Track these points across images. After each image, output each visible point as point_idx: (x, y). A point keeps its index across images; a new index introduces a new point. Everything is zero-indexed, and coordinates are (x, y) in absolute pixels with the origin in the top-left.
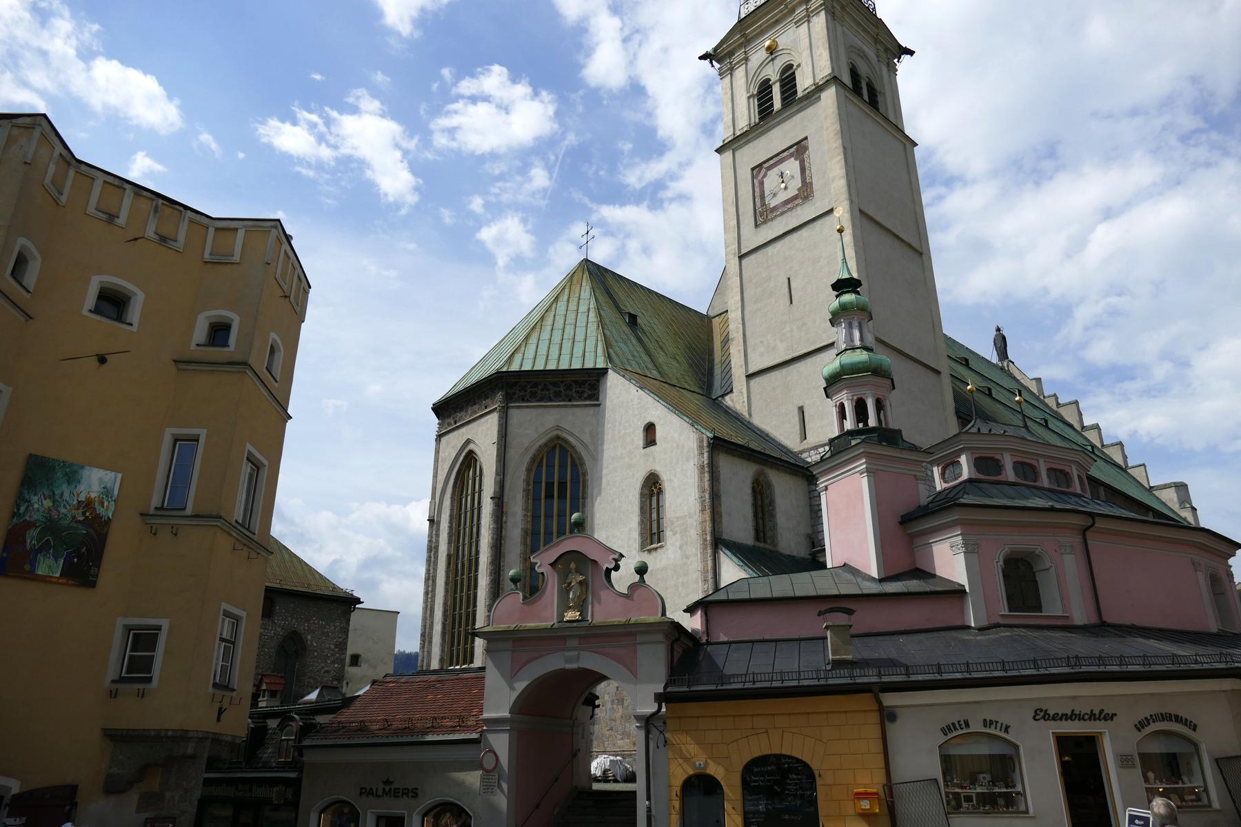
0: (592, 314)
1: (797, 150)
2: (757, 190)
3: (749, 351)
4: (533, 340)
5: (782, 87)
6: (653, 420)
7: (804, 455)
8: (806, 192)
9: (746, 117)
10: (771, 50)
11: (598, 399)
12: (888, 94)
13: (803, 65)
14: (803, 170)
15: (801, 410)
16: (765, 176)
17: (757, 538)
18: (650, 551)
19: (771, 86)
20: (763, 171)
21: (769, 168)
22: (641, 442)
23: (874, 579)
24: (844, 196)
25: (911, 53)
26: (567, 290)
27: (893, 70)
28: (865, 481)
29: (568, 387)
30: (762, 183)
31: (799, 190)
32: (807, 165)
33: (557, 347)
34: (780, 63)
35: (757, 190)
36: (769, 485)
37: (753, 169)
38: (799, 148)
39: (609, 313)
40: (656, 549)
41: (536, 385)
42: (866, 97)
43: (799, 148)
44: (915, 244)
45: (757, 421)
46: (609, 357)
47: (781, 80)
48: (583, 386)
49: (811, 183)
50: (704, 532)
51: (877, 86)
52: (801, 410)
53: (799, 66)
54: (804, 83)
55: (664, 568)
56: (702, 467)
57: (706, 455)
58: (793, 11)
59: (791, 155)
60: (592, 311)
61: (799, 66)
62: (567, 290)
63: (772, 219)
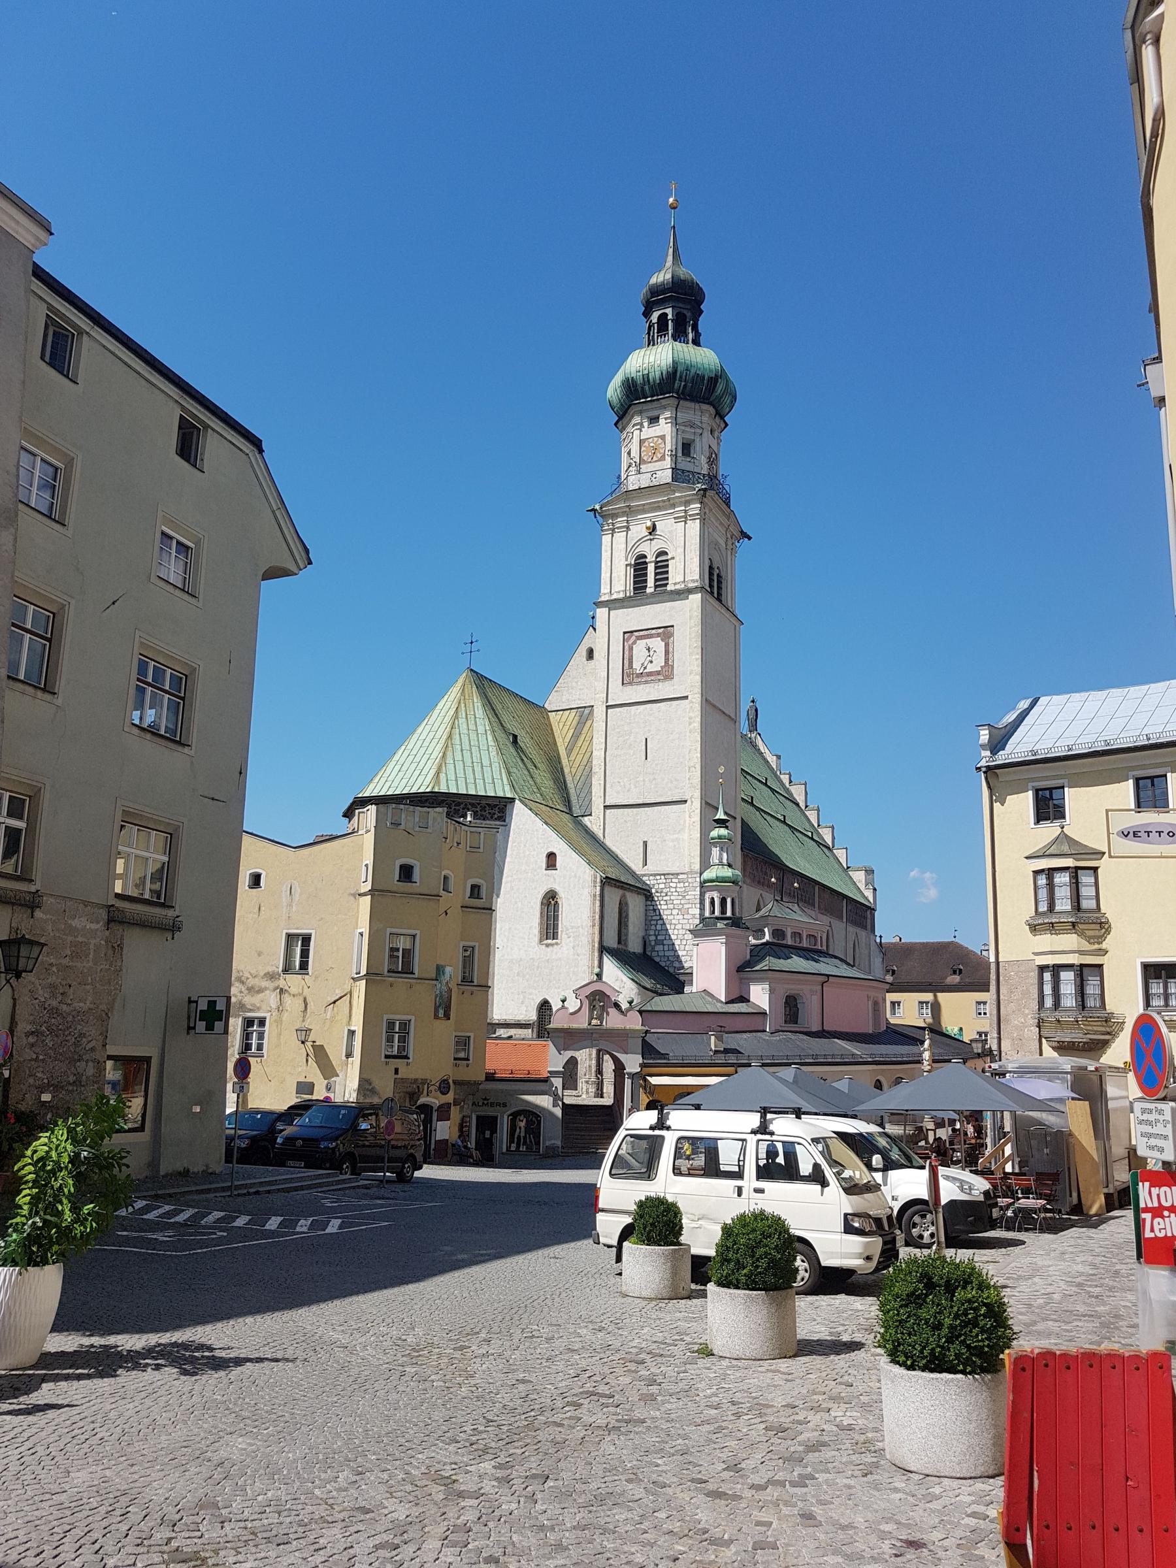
0: (490, 738)
2: (627, 653)
4: (449, 760)
5: (656, 568)
7: (645, 878)
8: (666, 673)
9: (623, 582)
10: (653, 530)
13: (677, 559)
14: (667, 652)
15: (645, 843)
16: (634, 643)
17: (619, 942)
18: (547, 945)
20: (633, 638)
21: (639, 638)
22: (544, 865)
24: (698, 690)
25: (750, 538)
27: (733, 551)
29: (483, 809)
30: (631, 649)
34: (657, 545)
35: (627, 653)
36: (627, 904)
40: (552, 945)
41: (459, 804)
44: (733, 716)
45: (609, 842)
47: (656, 562)
48: (495, 810)
50: (593, 941)
51: (723, 574)
52: (645, 843)
54: (675, 578)
56: (595, 896)
57: (598, 888)
58: (673, 506)
59: (658, 635)
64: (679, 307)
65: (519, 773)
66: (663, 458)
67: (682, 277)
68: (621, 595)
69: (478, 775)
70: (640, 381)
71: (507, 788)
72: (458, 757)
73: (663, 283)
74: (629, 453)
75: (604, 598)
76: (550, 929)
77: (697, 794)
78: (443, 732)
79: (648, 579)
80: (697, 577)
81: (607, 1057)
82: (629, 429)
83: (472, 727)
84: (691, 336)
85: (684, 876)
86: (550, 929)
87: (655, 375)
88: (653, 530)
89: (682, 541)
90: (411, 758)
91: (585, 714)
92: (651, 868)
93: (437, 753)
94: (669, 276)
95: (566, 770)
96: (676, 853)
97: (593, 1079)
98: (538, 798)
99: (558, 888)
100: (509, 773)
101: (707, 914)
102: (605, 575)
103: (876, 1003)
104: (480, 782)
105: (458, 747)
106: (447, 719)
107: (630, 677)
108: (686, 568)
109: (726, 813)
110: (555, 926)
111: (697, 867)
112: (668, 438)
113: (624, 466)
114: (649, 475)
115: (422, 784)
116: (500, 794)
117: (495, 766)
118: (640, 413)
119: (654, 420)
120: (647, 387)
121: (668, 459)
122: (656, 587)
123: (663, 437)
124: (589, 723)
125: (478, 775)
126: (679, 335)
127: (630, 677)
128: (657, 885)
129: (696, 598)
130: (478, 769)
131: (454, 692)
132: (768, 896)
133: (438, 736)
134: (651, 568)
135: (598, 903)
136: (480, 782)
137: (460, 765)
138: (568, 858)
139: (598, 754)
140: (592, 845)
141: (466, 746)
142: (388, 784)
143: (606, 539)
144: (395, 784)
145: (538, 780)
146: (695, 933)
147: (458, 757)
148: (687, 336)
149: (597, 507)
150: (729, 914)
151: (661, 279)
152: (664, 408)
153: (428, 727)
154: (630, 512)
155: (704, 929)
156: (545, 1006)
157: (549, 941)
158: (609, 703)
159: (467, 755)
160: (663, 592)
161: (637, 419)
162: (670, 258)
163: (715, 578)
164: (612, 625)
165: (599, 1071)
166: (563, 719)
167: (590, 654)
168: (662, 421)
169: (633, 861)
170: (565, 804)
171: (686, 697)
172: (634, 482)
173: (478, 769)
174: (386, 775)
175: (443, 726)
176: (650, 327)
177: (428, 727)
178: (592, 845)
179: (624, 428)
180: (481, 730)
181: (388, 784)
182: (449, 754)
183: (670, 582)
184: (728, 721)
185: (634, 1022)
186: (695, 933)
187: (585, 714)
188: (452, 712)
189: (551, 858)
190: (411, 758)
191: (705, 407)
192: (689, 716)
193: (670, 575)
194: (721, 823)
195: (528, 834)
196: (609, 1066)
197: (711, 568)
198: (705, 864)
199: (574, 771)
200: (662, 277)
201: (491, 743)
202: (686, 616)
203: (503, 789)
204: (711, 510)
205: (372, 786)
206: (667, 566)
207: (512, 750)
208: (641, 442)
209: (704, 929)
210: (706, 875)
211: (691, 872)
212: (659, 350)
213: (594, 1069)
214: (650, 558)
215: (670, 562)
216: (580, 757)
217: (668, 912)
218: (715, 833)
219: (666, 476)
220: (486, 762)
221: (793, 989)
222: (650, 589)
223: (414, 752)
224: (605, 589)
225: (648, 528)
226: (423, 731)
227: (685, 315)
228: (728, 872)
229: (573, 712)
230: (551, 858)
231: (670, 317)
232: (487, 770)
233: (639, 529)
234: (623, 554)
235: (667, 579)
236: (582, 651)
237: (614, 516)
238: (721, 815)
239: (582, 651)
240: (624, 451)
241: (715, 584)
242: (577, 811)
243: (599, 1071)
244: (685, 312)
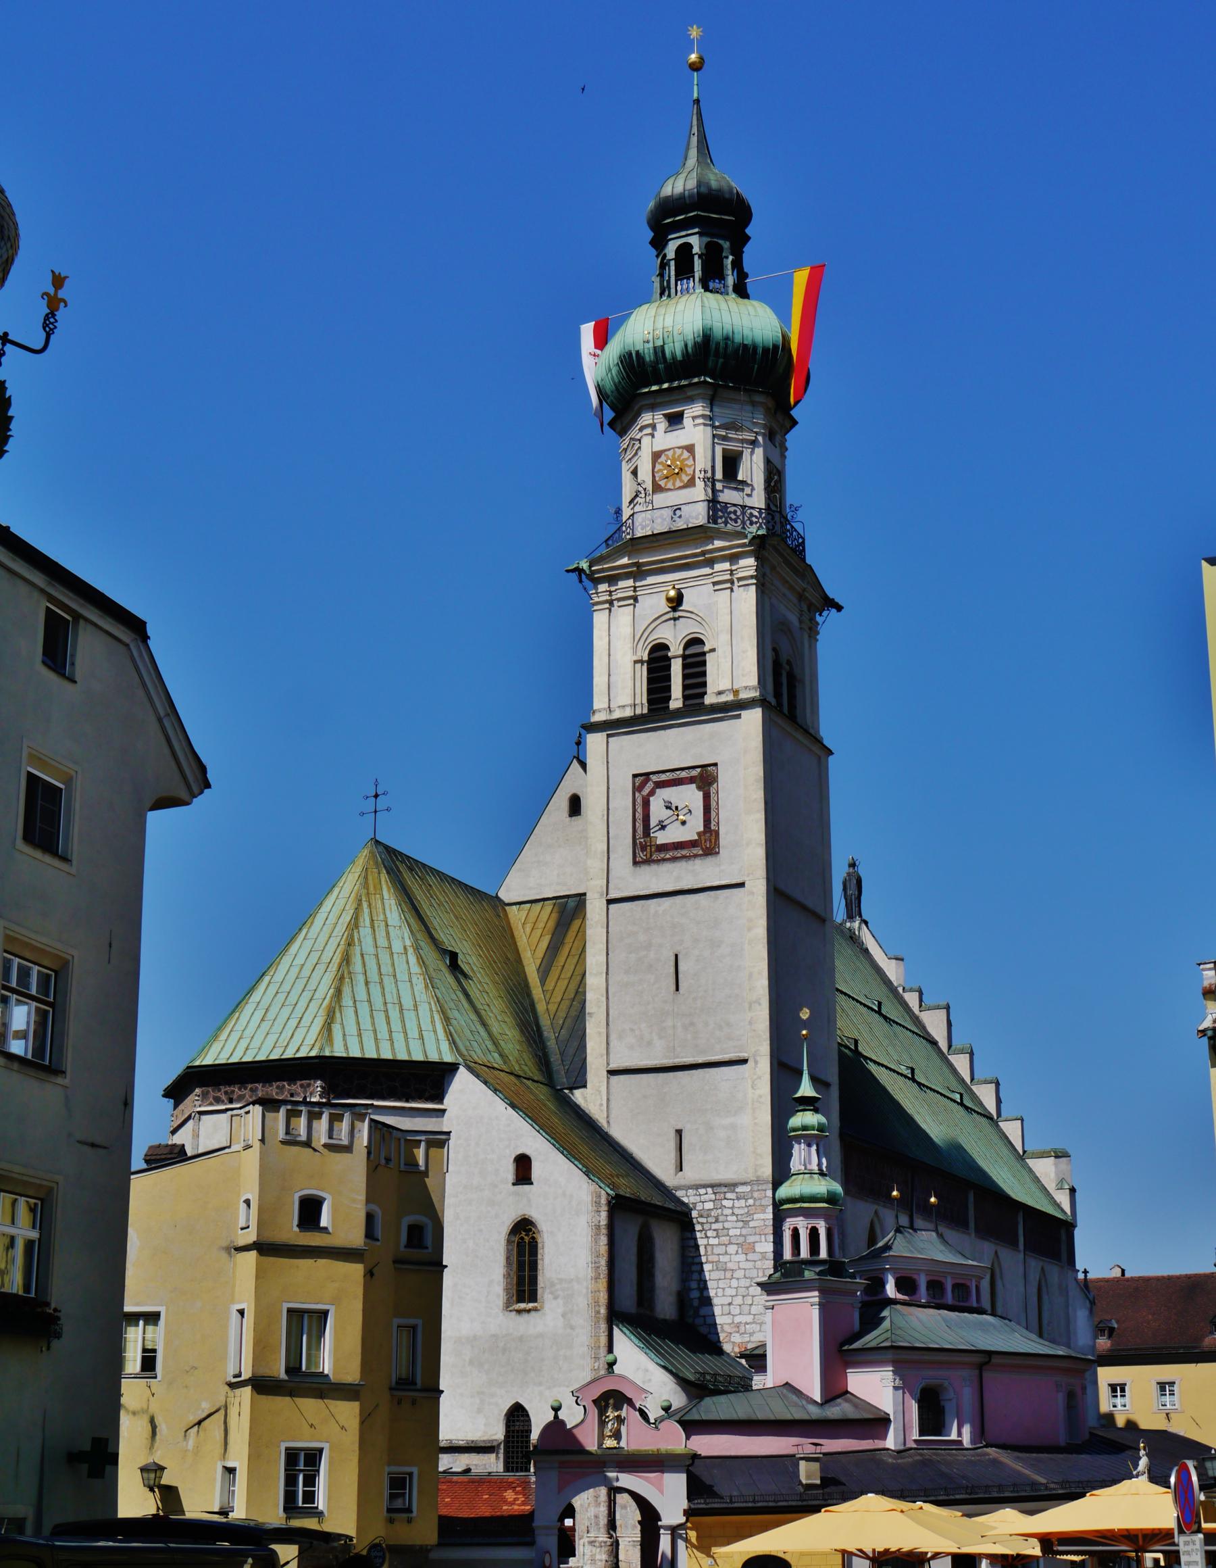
0: (413, 959)
1: (701, 774)
3: (613, 1037)
4: (347, 1000)
5: (685, 666)
6: (528, 1152)
8: (707, 843)
9: (629, 691)
11: (441, 1101)
12: (807, 683)
13: (719, 651)
16: (652, 793)
19: (669, 659)
20: (650, 785)
23: (816, 1402)
26: (365, 905)
28: (815, 1313)
30: (646, 804)
31: (699, 834)
32: (713, 804)
33: (382, 1015)
35: (640, 810)
37: (635, 776)
38: (705, 777)
39: (425, 945)
42: (786, 710)
43: (705, 777)
46: (453, 1043)
47: (684, 657)
49: (717, 833)
50: (597, 1303)
53: (713, 650)
55: (541, 1336)
56: (598, 1227)
58: (710, 563)
59: (691, 780)
60: (410, 951)
61: (713, 650)
62: (365, 905)
63: (658, 861)
64: (710, 234)
65: (463, 1019)
66: (691, 483)
67: (714, 185)
68: (628, 713)
69: (396, 1025)
70: (649, 357)
71: (445, 1046)
72: (361, 993)
73: (682, 197)
74: (635, 473)
75: (598, 717)
76: (524, 1285)
77: (765, 1048)
78: (333, 952)
79: (674, 686)
80: (754, 681)
81: (623, 1499)
82: (634, 433)
83: (382, 942)
84: (730, 280)
85: (747, 1189)
86: (524, 1285)
87: (675, 348)
88: (676, 602)
89: (727, 620)
90: (281, 997)
91: (570, 910)
92: (691, 1173)
93: (325, 988)
94: (692, 184)
95: (541, 1007)
96: (726, 1145)
97: (603, 1537)
98: (495, 1059)
99: (535, 1215)
100: (447, 1020)
101: (787, 1255)
102: (599, 680)
103: (1071, 1396)
104: (399, 1038)
105: (361, 978)
106: (341, 928)
107: (646, 850)
108: (735, 667)
109: (814, 1080)
110: (534, 1280)
111: (767, 1171)
112: (699, 451)
113: (627, 495)
114: (669, 512)
115: (302, 1043)
116: (433, 1057)
117: (424, 1009)
118: (653, 408)
119: (675, 420)
120: (661, 366)
121: (700, 484)
122: (685, 698)
123: (690, 449)
124: (576, 924)
125: (396, 1025)
126: (712, 278)
127: (646, 850)
128: (700, 1202)
129: (753, 718)
130: (394, 1014)
131: (349, 883)
132: (888, 1217)
133: (326, 959)
134: (676, 668)
135: (604, 1240)
136: (399, 1038)
137: (364, 1009)
138: (551, 1164)
139: (594, 983)
140: (588, 1142)
141: (373, 976)
142: (243, 1044)
143: (600, 619)
144: (256, 1043)
145: (496, 1028)
146: (769, 1287)
147: (361, 993)
148: (722, 277)
149: (584, 565)
150: (823, 1254)
151: (679, 189)
152: (691, 400)
153: (308, 944)
154: (639, 572)
155: (784, 1278)
156: (517, 1416)
157: (522, 1306)
158: (612, 895)
159: (375, 990)
160: (697, 707)
161: (646, 418)
162: (693, 152)
163: (784, 680)
164: (610, 766)
165: (612, 1525)
166: (532, 918)
167: (575, 806)
168: (687, 421)
169: (659, 1164)
170: (547, 1076)
171: (742, 885)
172: (644, 526)
173: (394, 1014)
174: (240, 1027)
175: (333, 942)
176: (664, 265)
177: (308, 944)
178: (588, 1142)
179: (622, 433)
180: (397, 947)
181: (243, 1044)
182: (346, 990)
183: (711, 688)
184: (805, 916)
185: (673, 1440)
186: (769, 1287)
187: (570, 910)
188: (347, 917)
189: (523, 1169)
190: (281, 997)
191: (759, 398)
192: (750, 913)
193: (709, 679)
194: (808, 1103)
195: (478, 1125)
196: (628, 1515)
197: (777, 665)
198: (781, 1173)
199: (553, 1008)
200: (679, 185)
201: (415, 969)
202: (738, 748)
203: (438, 1050)
204: (773, 568)
205: (216, 1047)
206: (704, 663)
207: (450, 979)
208: (656, 456)
209: (784, 1278)
210: (784, 1191)
211: (758, 1181)
212: (680, 307)
213: (603, 1521)
214: (676, 649)
215: (708, 657)
216: (562, 985)
217: (721, 1250)
218: (797, 1120)
219: (697, 515)
220: (407, 1002)
221: (930, 1376)
222: (676, 702)
223: (286, 987)
224: (599, 702)
225: (669, 600)
226: (299, 950)
227: (721, 248)
228: (821, 1186)
229: (549, 906)
230: (523, 1169)
231: (696, 250)
232: (410, 1016)
233: (654, 603)
234: (628, 645)
235: (704, 684)
236: (560, 802)
237: (612, 580)
238: (806, 1089)
239: (560, 802)
240: (626, 476)
241: (786, 692)
242: (562, 1079)
243: (612, 1525)
244: (721, 242)
